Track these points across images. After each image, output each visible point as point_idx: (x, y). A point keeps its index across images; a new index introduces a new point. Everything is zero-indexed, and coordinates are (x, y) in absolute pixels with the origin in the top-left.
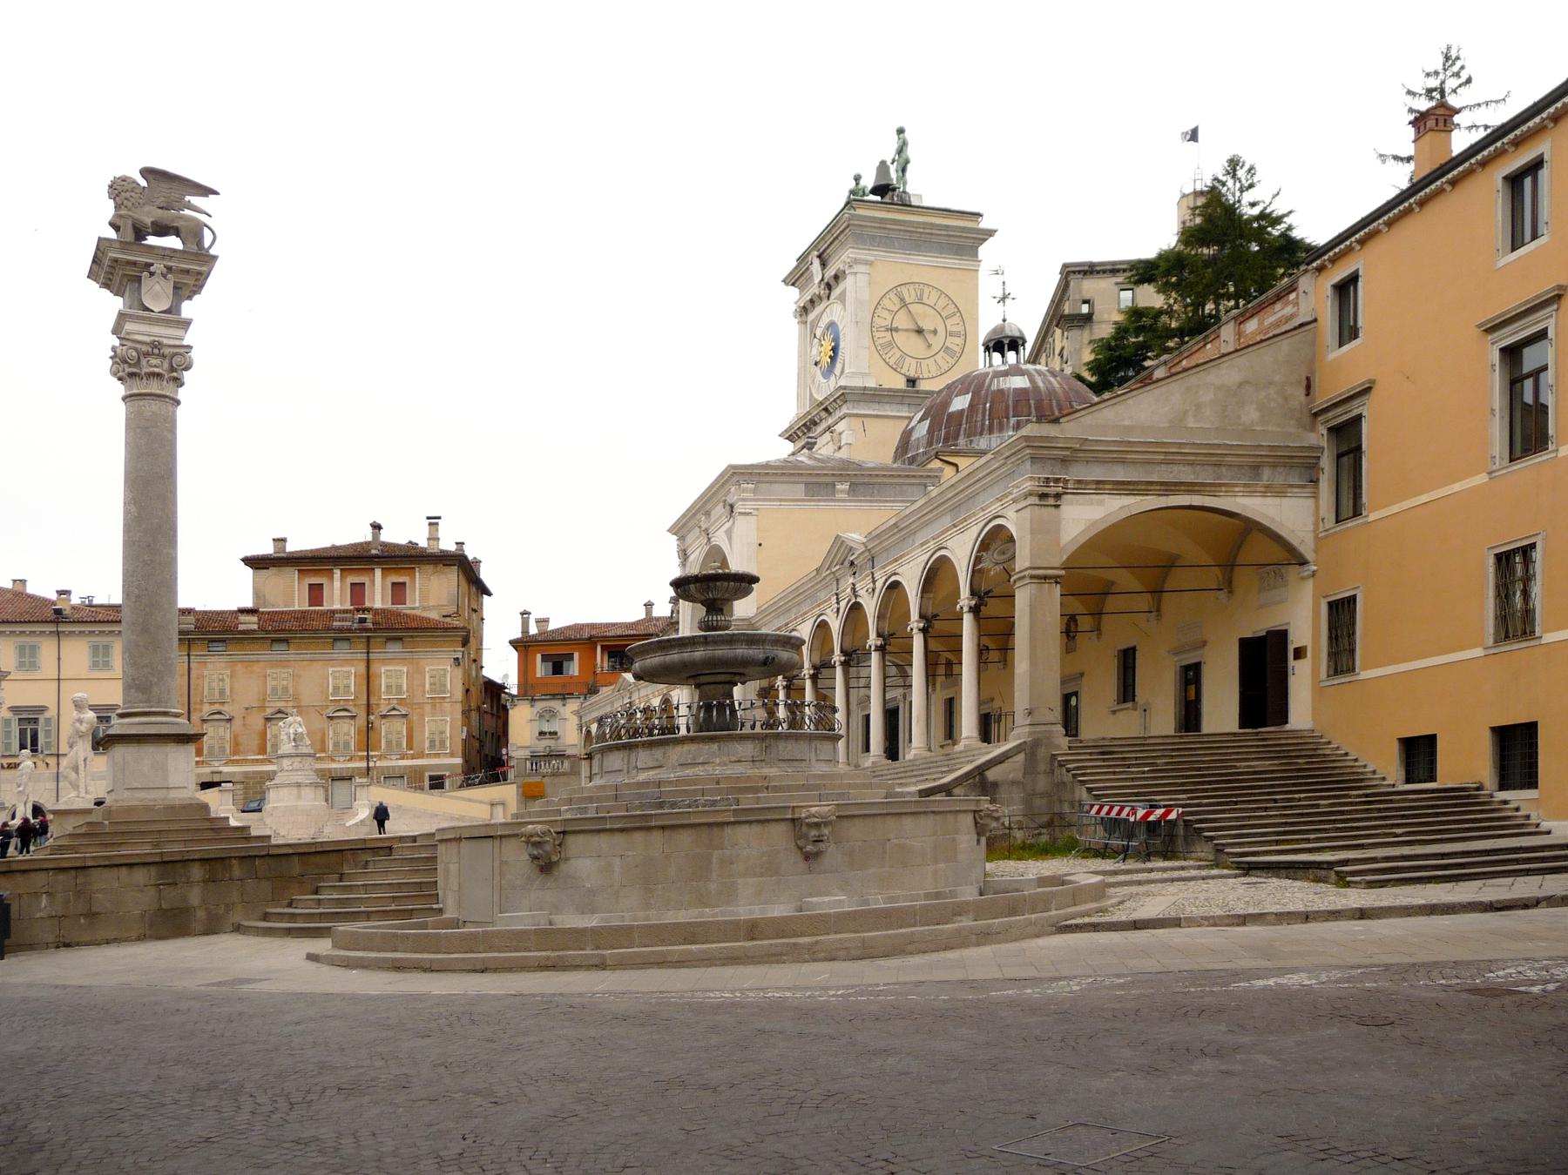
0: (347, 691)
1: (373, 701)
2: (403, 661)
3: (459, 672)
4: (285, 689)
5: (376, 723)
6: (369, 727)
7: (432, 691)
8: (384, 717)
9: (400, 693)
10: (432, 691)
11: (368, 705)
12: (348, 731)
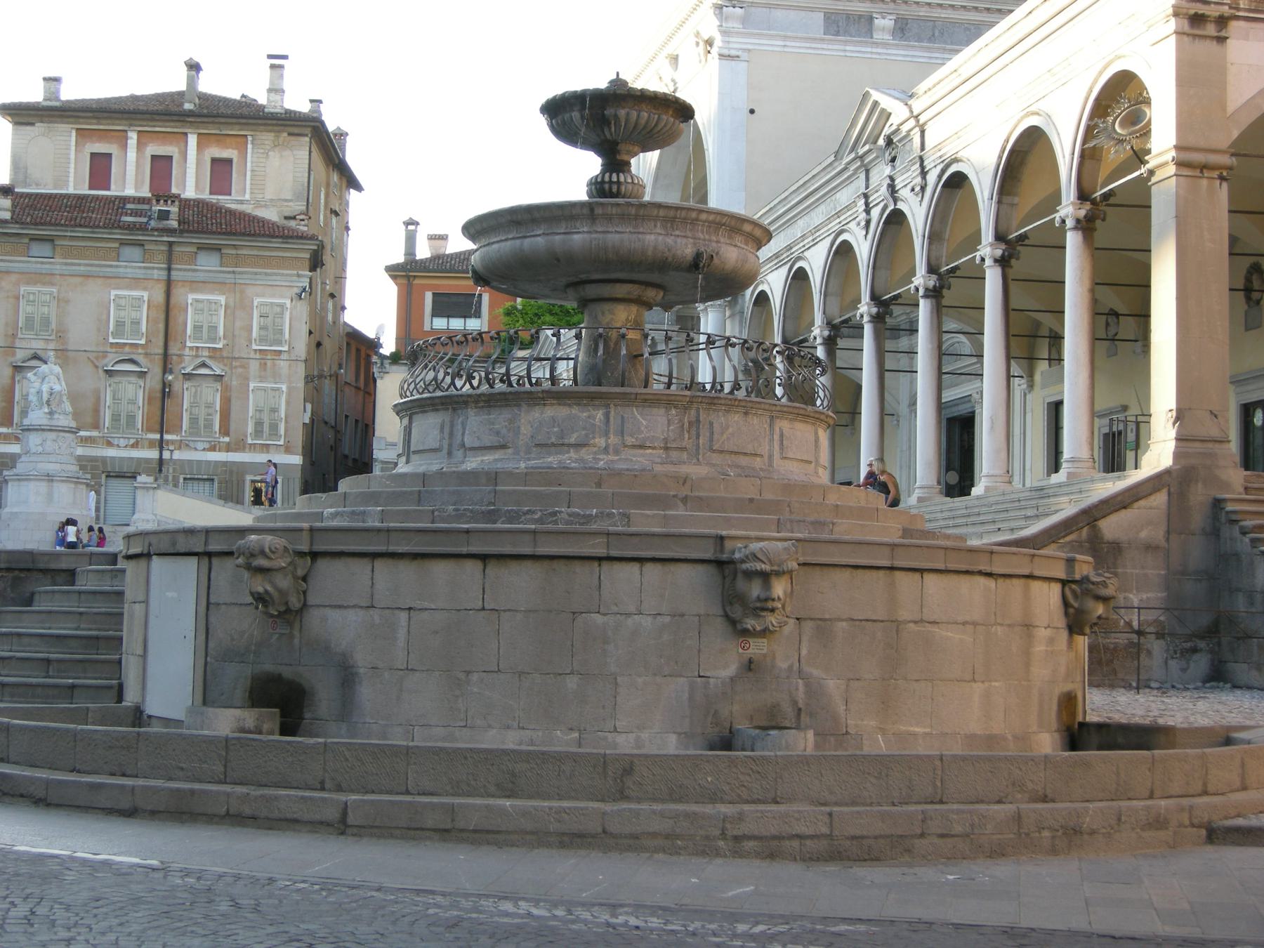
0: (136, 332)
1: (173, 350)
2: (219, 286)
3: (303, 309)
4: (46, 321)
5: (177, 387)
6: (166, 392)
7: (262, 340)
8: (188, 376)
9: (214, 340)
10: (262, 340)
11: (166, 356)
12: (134, 395)
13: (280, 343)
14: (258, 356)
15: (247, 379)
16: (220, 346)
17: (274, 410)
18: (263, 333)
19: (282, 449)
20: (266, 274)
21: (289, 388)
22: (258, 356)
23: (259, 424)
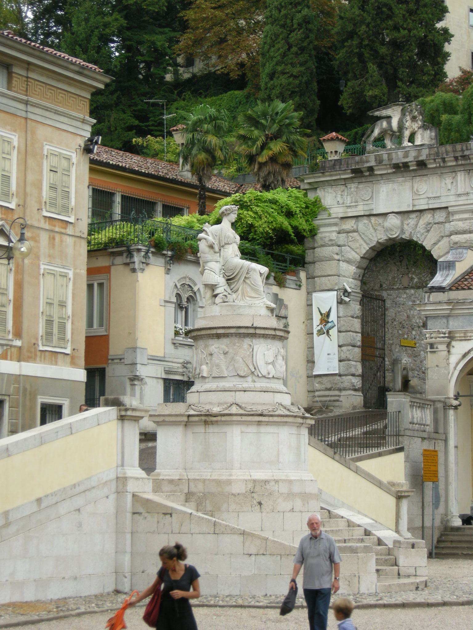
7: (53, 204)
13: (66, 209)
14: (47, 226)
15: (38, 257)
16: (12, 206)
17: (62, 305)
18: (53, 195)
19: (68, 359)
20: (57, 112)
21: (75, 274)
22: (47, 226)
23: (49, 322)
